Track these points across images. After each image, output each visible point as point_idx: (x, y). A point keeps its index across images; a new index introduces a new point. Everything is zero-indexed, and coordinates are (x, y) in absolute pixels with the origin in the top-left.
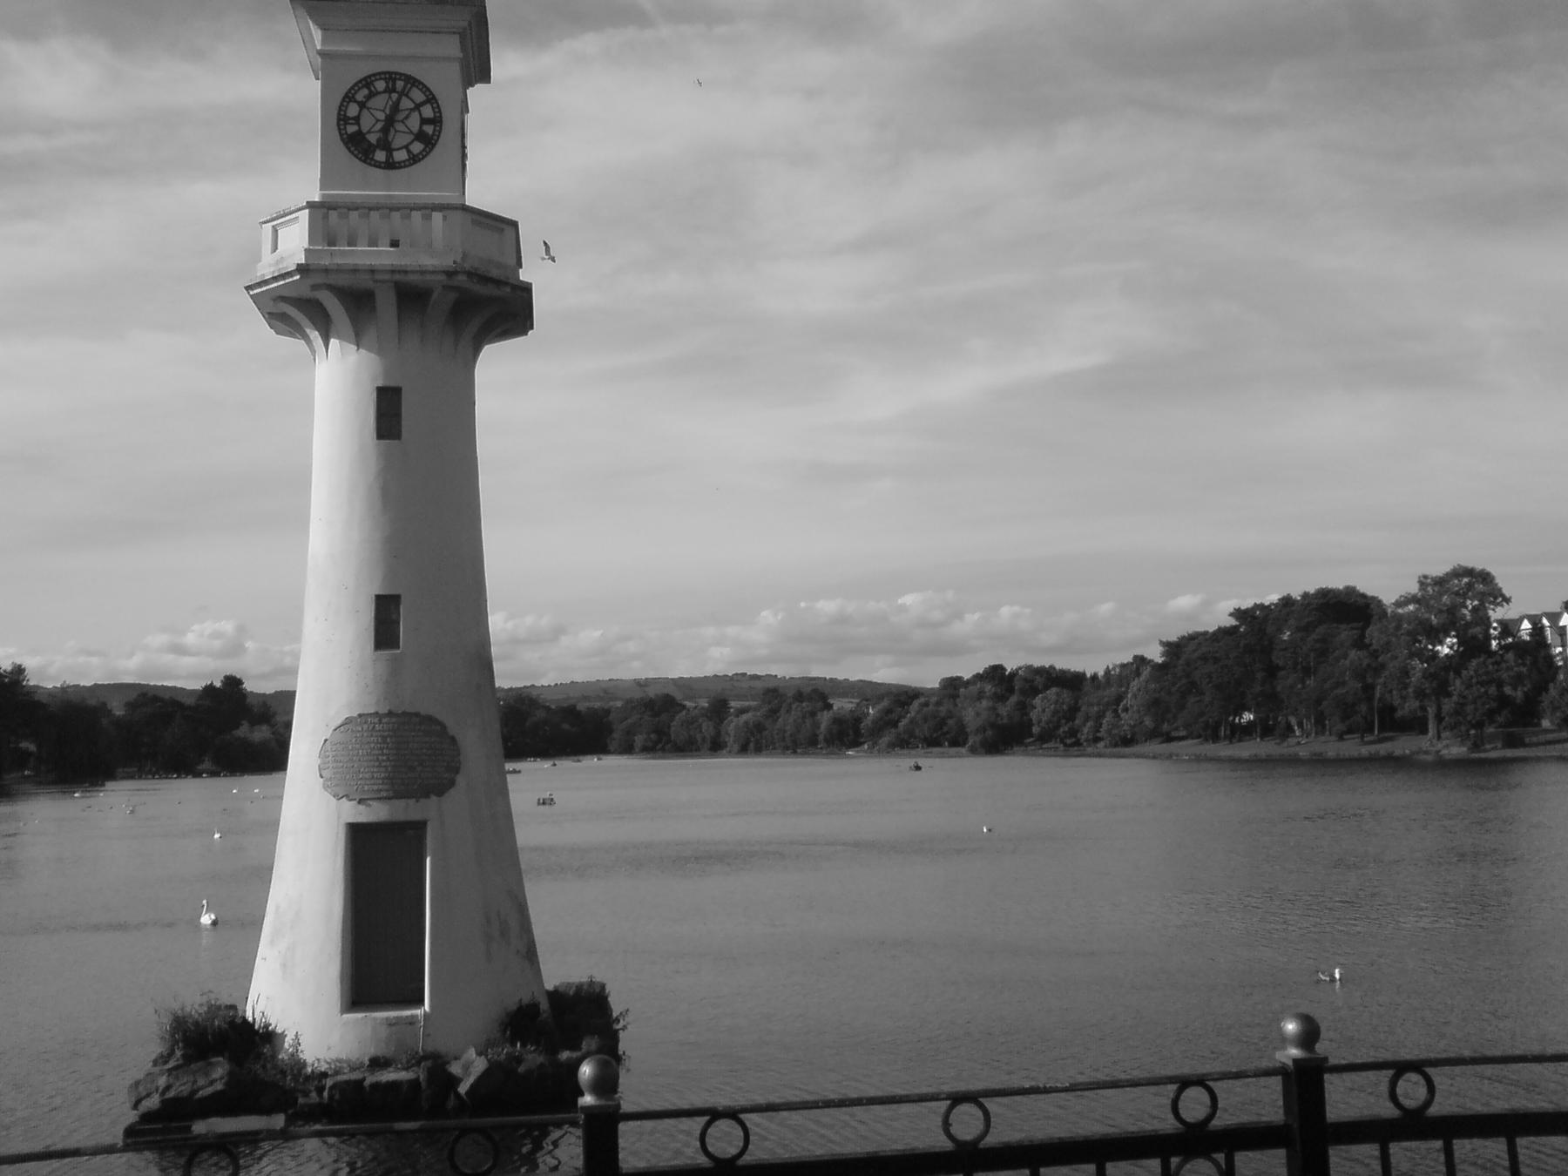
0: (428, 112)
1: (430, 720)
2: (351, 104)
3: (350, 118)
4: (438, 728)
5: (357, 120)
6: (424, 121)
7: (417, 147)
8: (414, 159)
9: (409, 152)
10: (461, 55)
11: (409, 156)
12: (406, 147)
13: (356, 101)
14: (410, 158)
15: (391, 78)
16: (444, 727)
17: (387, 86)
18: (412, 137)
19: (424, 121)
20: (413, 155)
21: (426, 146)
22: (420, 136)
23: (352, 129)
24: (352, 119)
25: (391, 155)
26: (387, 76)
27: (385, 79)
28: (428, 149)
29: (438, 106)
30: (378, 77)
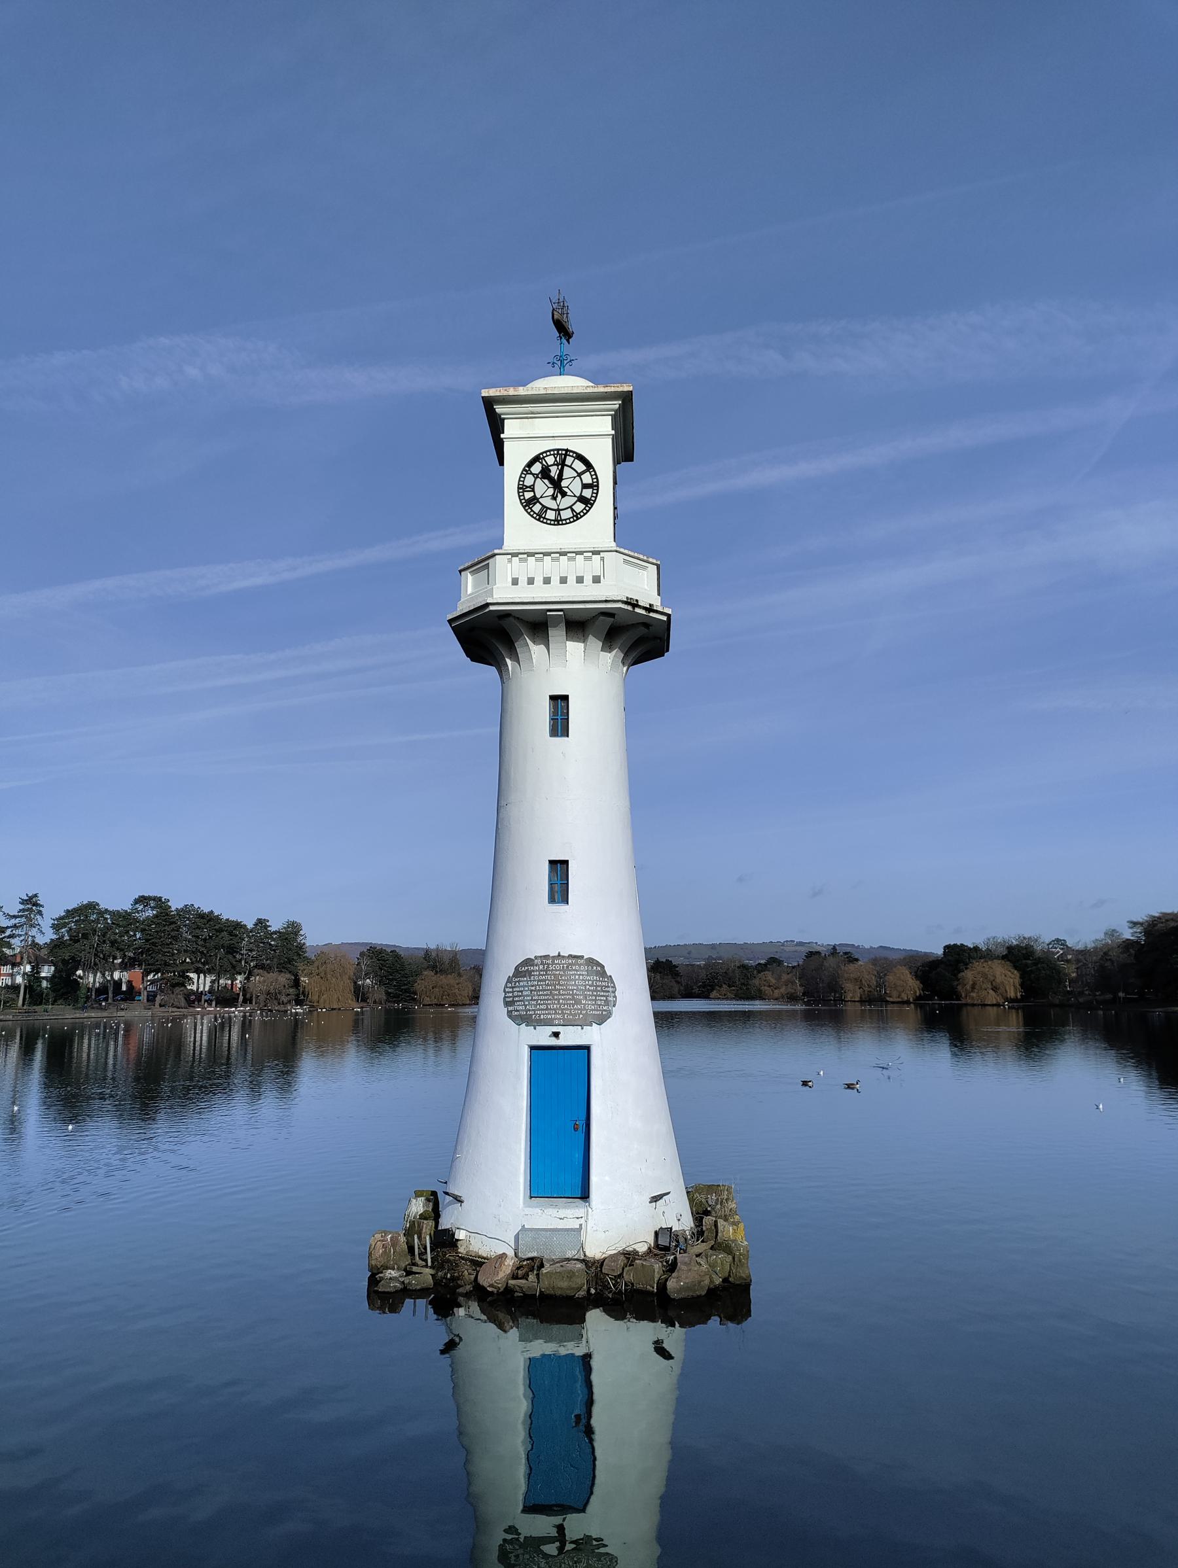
0: (587, 479)
1: (591, 962)
2: (527, 475)
3: (527, 487)
4: (599, 968)
5: (532, 487)
6: (585, 486)
7: (579, 507)
8: (577, 517)
9: (573, 510)
10: (613, 432)
11: (573, 514)
12: (571, 507)
13: (531, 473)
14: (574, 516)
15: (558, 454)
16: (602, 967)
17: (556, 460)
18: (576, 499)
21: (587, 506)
22: (582, 499)
23: (528, 495)
24: (530, 487)
25: (559, 514)
26: (556, 452)
27: (554, 455)
28: (587, 508)
29: (596, 474)
30: (548, 453)
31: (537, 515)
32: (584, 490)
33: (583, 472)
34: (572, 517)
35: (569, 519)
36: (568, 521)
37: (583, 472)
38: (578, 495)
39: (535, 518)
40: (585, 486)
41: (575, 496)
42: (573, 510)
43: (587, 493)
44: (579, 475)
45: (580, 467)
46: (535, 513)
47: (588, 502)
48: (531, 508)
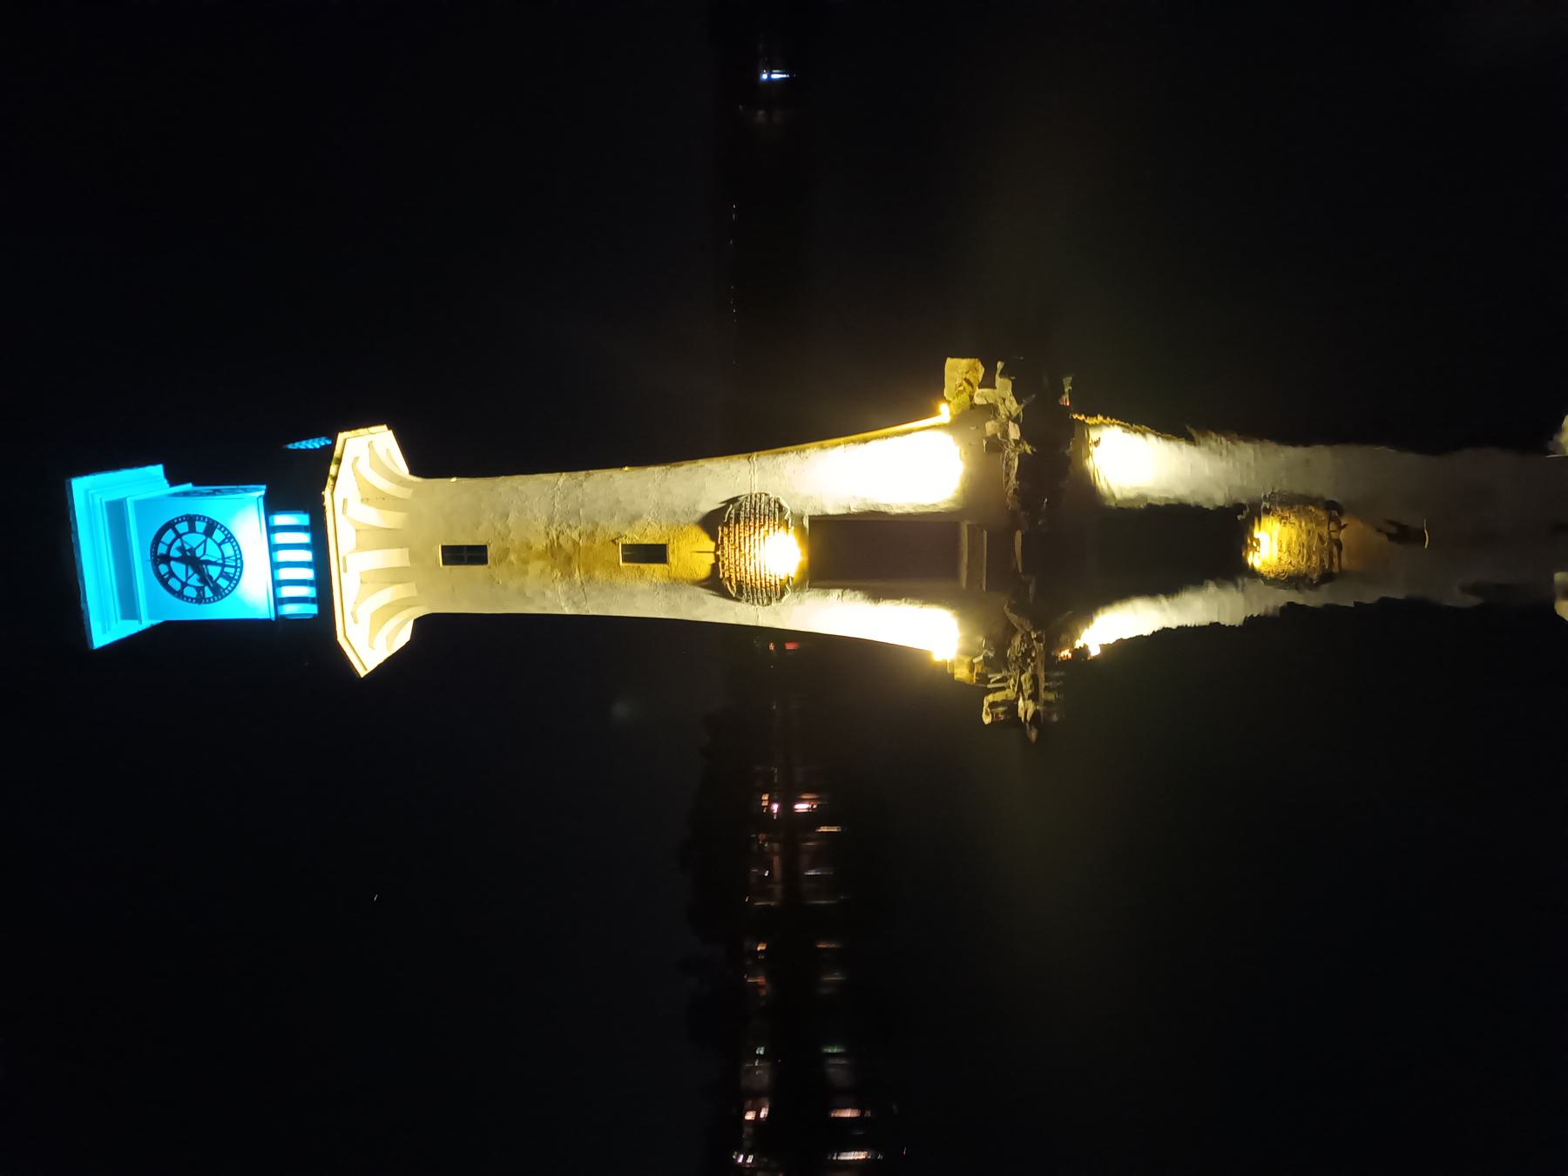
3: (199, 594)
7: (218, 535)
8: (229, 538)
9: (223, 542)
12: (219, 545)
19: (192, 530)
20: (226, 538)
25: (229, 558)
31: (231, 582)
32: (197, 530)
33: (175, 531)
34: (232, 543)
35: (233, 547)
36: (236, 548)
37: (175, 531)
38: (203, 537)
39: (236, 585)
40: (192, 530)
41: (205, 541)
42: (223, 542)
43: (201, 526)
44: (179, 536)
45: (169, 536)
46: (229, 585)
47: (211, 527)
48: (224, 590)
